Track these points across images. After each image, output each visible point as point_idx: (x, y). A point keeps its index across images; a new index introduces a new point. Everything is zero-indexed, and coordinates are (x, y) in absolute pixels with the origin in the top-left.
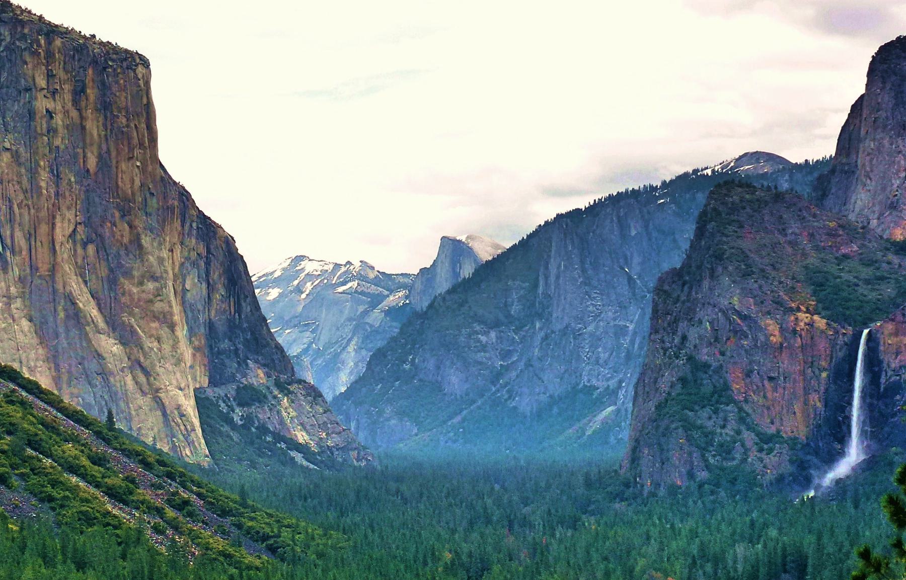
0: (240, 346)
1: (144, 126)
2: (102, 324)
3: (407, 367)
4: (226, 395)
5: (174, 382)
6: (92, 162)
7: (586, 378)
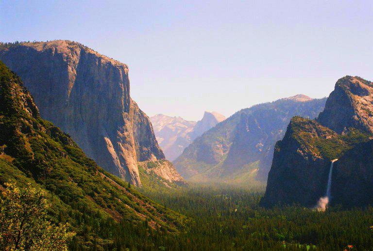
2: (111, 144)
6: (110, 95)
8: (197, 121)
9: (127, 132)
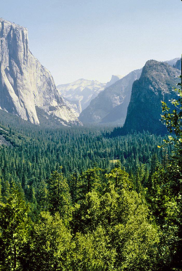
1: (25, 44)
8: (107, 83)
9: (25, 81)
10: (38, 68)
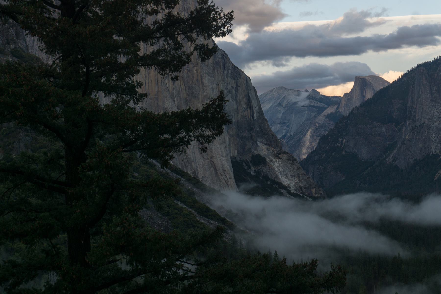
0: (254, 134)
3: (339, 145)
4: (246, 160)
5: (221, 153)
7: (433, 151)
10: (226, 72)
